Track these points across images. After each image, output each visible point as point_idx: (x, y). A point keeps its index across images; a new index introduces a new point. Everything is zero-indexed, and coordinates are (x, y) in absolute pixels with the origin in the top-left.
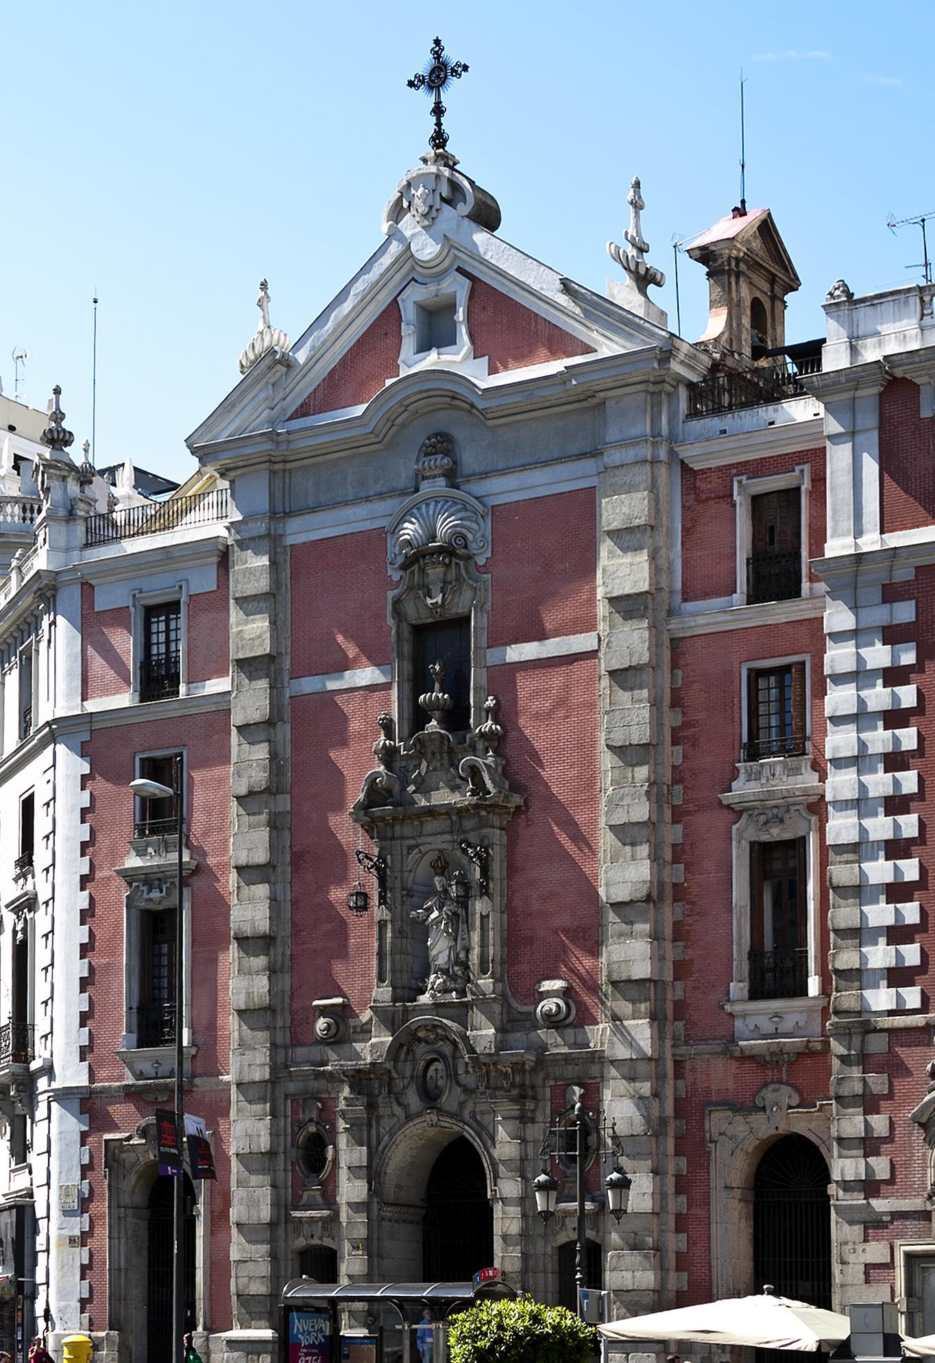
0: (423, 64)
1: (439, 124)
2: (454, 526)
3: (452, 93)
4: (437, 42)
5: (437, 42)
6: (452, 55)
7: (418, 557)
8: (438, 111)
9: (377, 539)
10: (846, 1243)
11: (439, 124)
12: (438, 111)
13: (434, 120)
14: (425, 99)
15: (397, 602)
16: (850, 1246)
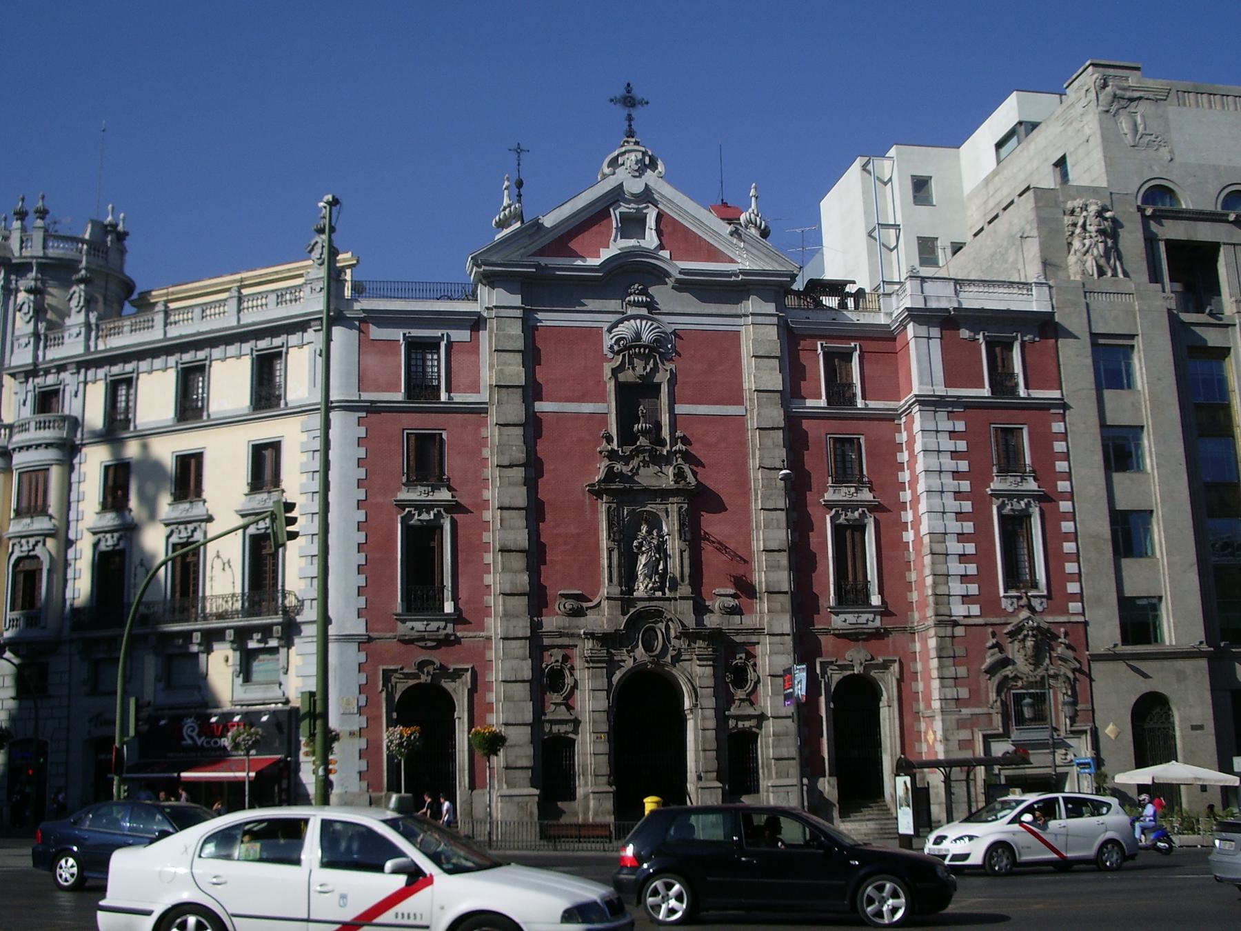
0: (620, 91)
1: (630, 126)
2: (661, 336)
3: (636, 113)
4: (629, 85)
5: (629, 85)
6: (638, 93)
7: (630, 349)
8: (630, 118)
9: (592, 335)
10: (948, 730)
11: (630, 126)
12: (630, 118)
13: (627, 123)
14: (623, 112)
15: (615, 372)
16: (951, 732)
